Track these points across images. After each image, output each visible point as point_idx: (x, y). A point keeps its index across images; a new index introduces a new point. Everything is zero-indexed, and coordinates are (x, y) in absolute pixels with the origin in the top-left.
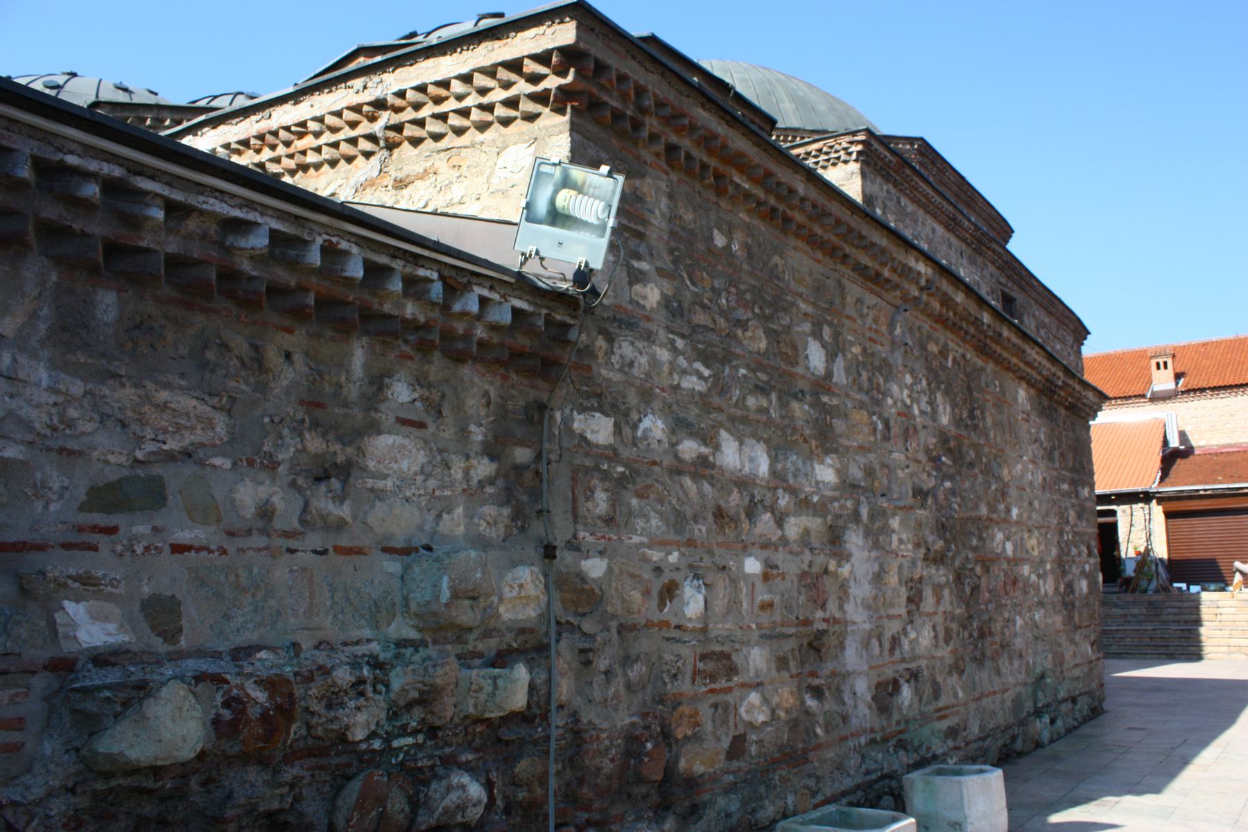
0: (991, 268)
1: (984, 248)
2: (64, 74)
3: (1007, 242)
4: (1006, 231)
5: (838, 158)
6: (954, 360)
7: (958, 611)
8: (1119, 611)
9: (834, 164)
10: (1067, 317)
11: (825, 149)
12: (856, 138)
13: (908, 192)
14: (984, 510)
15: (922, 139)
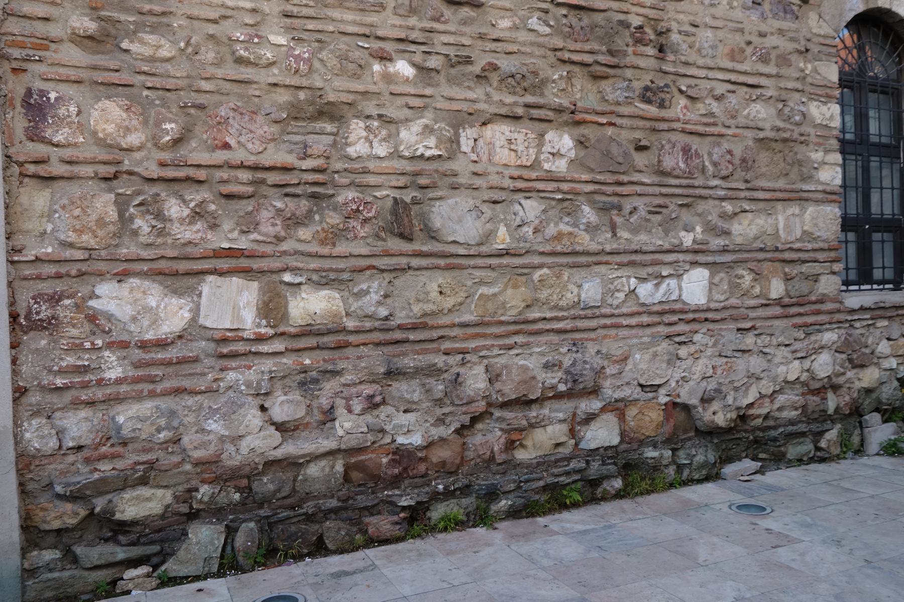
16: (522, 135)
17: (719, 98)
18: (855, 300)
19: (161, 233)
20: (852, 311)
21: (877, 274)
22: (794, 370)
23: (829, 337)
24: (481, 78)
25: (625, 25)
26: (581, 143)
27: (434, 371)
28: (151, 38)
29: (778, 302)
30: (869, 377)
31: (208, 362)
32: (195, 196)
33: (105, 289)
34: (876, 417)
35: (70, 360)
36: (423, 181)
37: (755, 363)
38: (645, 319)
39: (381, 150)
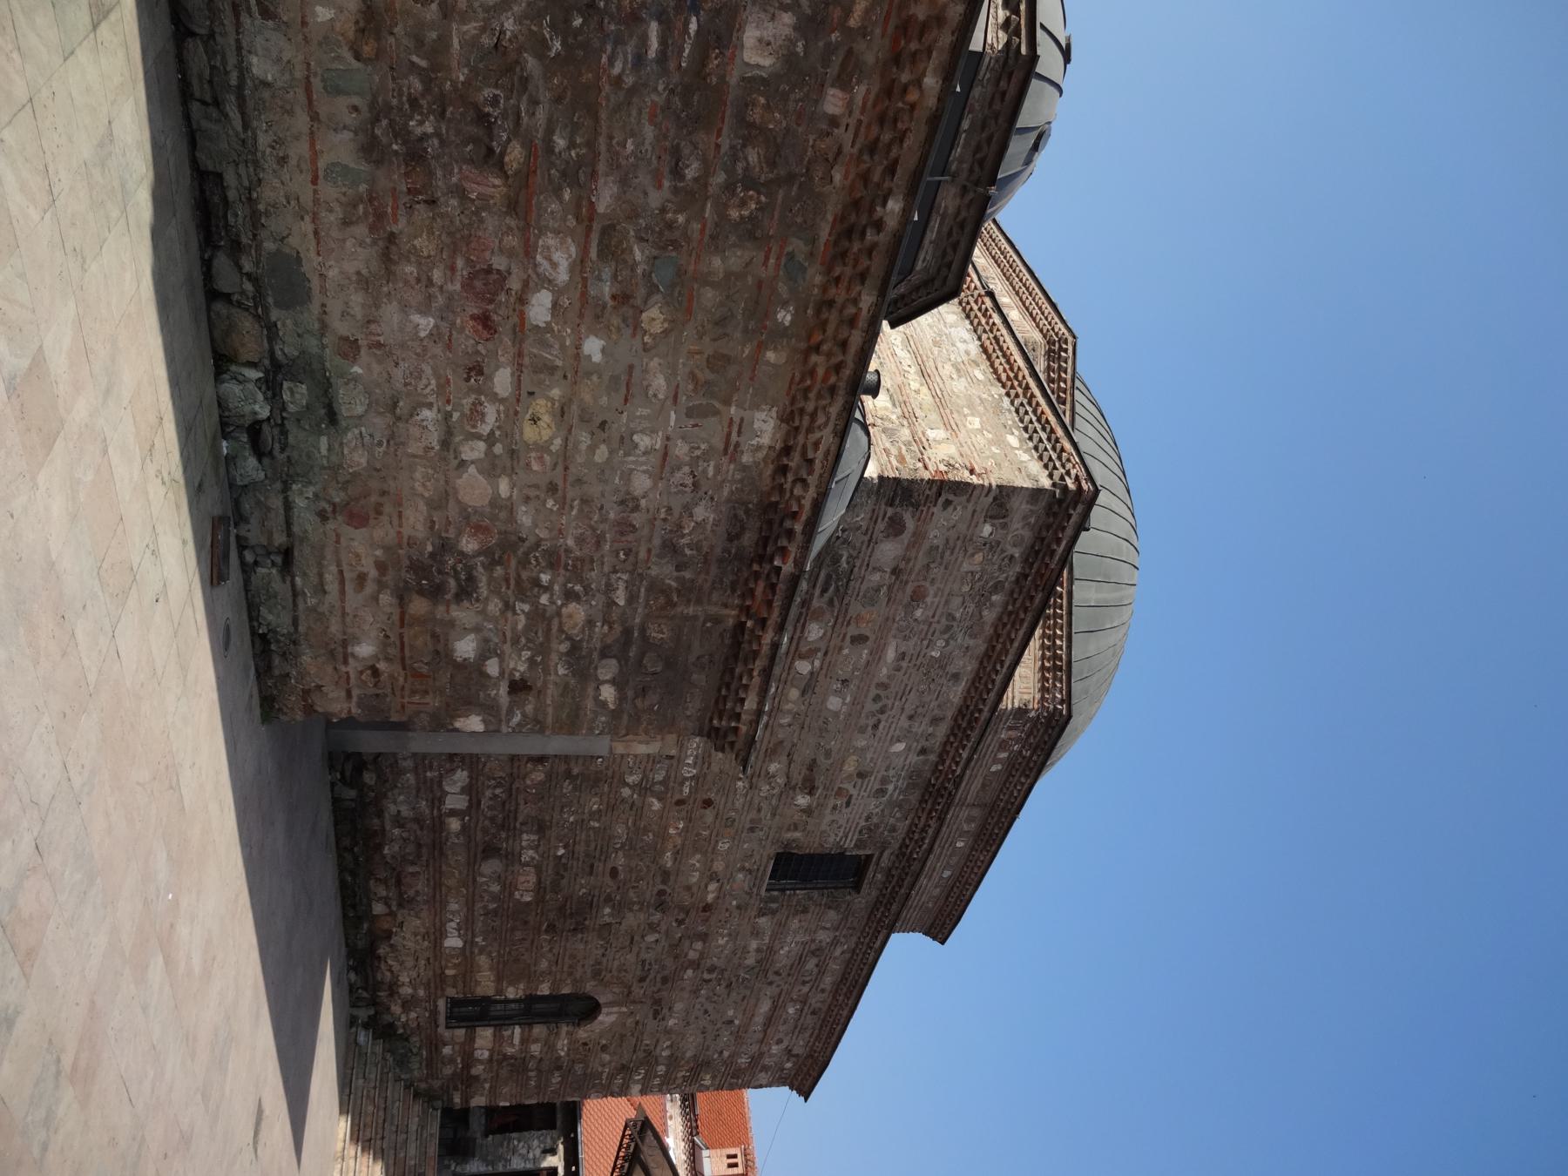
0: (903, 827)
1: (929, 806)
2: (1068, 39)
3: (926, 934)
4: (940, 927)
5: (1055, 468)
6: (834, 121)
7: (456, 42)
8: (413, 1127)
9: (1046, 466)
10: (831, 1033)
11: (1064, 454)
12: (1083, 483)
13: (1010, 608)
14: (605, 197)
15: (1070, 716)
16: (531, 885)
17: (551, 950)
18: (441, 1004)
19: (489, 787)
20: (435, 1002)
21: (456, 1010)
22: (404, 978)
23: (421, 993)
24: (557, 873)
25: (585, 919)
26: (528, 904)
27: (419, 856)
28: (570, 787)
29: (443, 973)
30: (396, 1009)
31: (431, 796)
32: (504, 796)
33: (465, 773)
34: (372, 1012)
35: (435, 764)
36: (510, 857)
37: (410, 963)
38: (438, 924)
39: (524, 844)
